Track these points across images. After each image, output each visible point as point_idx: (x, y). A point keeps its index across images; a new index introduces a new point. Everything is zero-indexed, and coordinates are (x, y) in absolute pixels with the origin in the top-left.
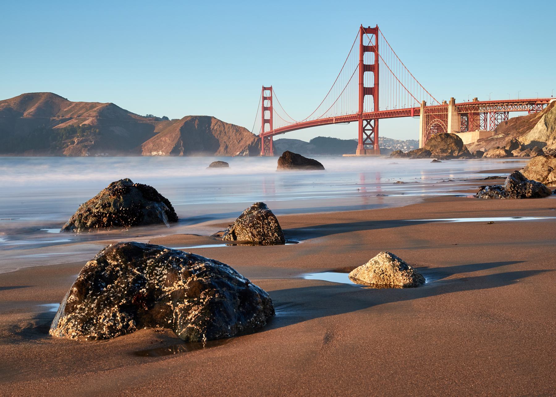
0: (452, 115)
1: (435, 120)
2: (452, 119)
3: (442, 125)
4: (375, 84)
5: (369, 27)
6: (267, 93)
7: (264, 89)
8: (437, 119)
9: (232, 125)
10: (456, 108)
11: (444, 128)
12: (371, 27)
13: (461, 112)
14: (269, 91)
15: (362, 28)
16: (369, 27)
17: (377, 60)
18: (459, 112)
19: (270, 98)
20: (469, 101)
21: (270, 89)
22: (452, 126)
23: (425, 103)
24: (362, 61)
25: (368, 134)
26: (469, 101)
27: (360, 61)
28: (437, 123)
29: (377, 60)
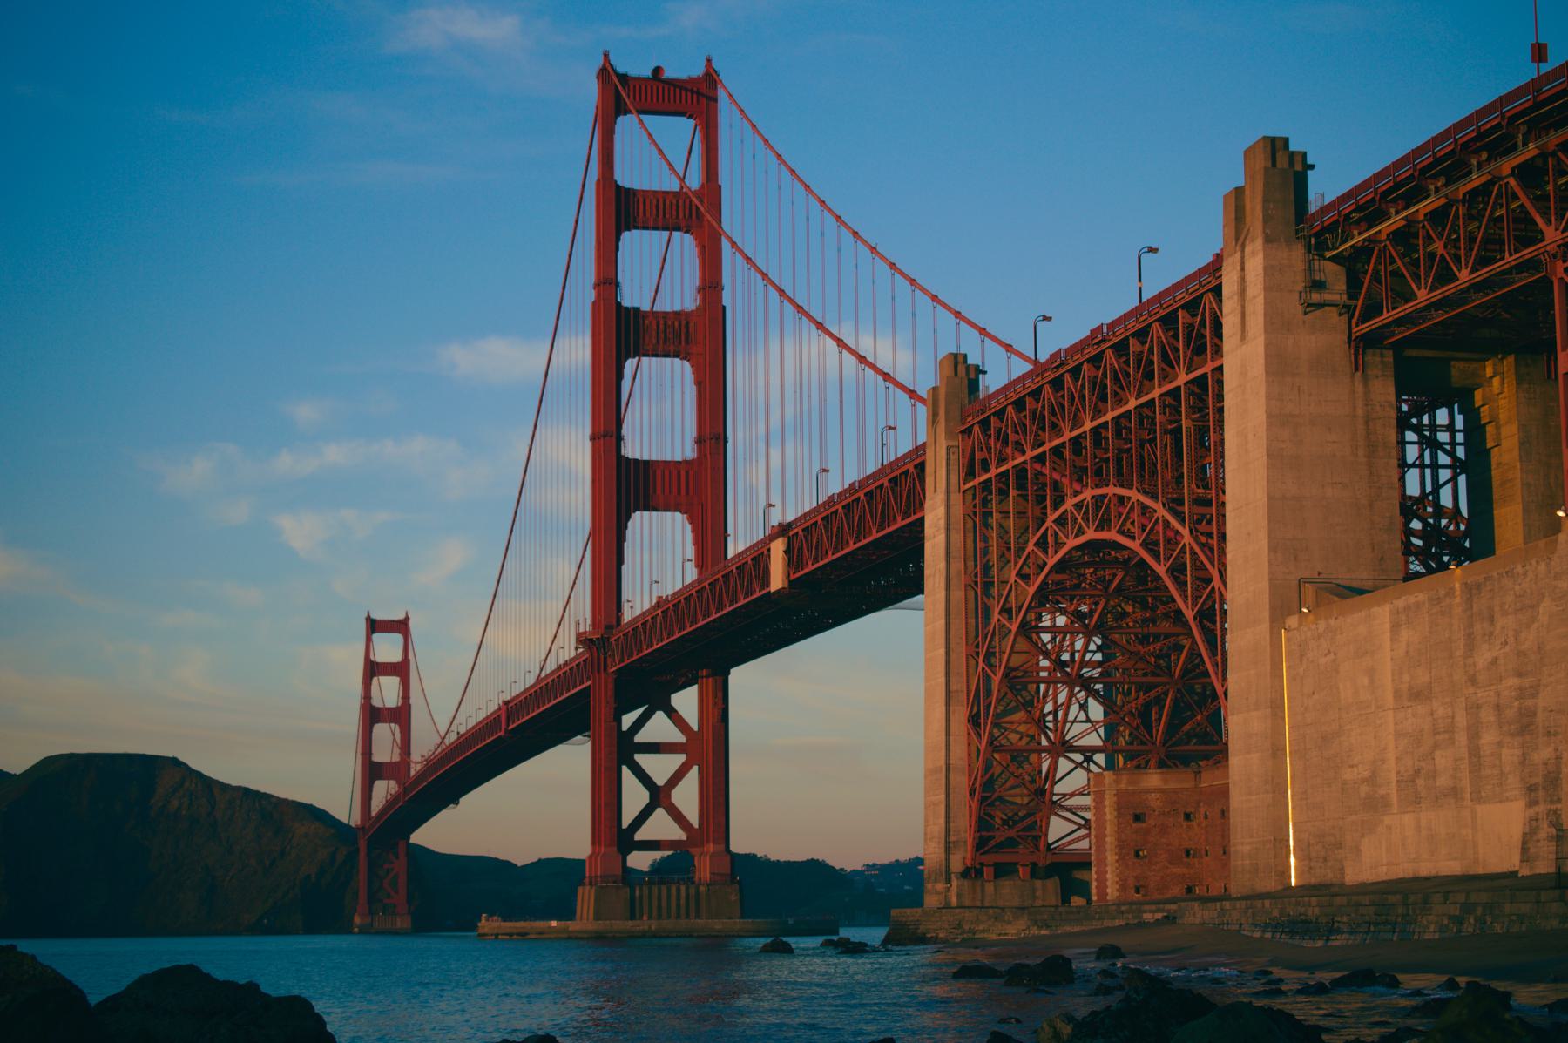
0: (1278, 364)
1: (1069, 504)
2: (1277, 419)
3: (1150, 545)
4: (699, 441)
5: (657, 71)
6: (388, 649)
7: (374, 626)
8: (1087, 494)
9: (246, 792)
10: (1334, 275)
11: (1177, 571)
12: (668, 74)
13: (1409, 297)
14: (398, 638)
15: (607, 74)
16: (657, 71)
17: (711, 285)
18: (1372, 310)
19: (401, 670)
20: (1539, 52)
21: (401, 627)
22: (1280, 508)
23: (963, 373)
24: (607, 282)
25: (660, 781)
26: (1539, 52)
27: (597, 285)
28: (1091, 534)
29: (711, 285)
